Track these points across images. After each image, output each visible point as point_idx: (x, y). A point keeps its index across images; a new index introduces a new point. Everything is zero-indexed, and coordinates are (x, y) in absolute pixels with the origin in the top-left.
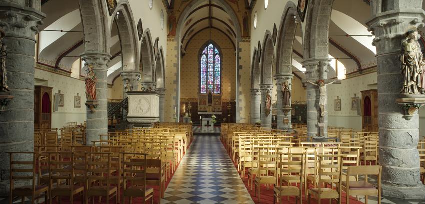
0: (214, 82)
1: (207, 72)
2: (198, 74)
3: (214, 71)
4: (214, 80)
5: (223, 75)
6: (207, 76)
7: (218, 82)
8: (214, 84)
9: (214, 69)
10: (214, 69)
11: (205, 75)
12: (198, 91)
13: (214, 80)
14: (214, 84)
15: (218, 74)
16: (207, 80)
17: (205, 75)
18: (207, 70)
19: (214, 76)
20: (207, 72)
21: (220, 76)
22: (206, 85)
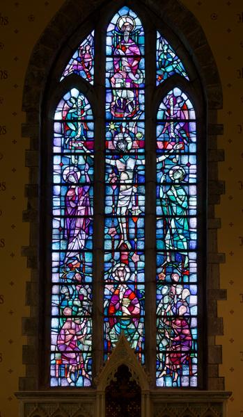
0: (148, 299)
1: (96, 224)
2: (23, 234)
3: (149, 215)
4: (153, 282)
5: (228, 242)
6: (98, 251)
7: (189, 299)
8: (150, 317)
9: (152, 200)
10: (152, 200)
11: (77, 244)
12: (21, 370)
13: (153, 282)
14: (150, 317)
15: (184, 234)
16: (98, 285)
17: (77, 244)
18: (99, 202)
19: (151, 252)
20: (96, 224)
21: (201, 249)
22: (86, 327)
